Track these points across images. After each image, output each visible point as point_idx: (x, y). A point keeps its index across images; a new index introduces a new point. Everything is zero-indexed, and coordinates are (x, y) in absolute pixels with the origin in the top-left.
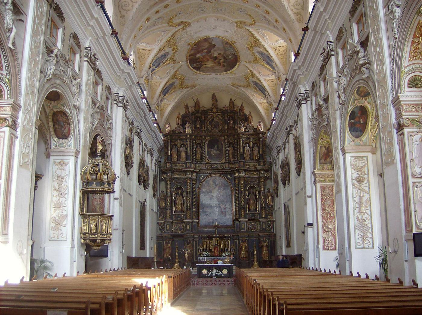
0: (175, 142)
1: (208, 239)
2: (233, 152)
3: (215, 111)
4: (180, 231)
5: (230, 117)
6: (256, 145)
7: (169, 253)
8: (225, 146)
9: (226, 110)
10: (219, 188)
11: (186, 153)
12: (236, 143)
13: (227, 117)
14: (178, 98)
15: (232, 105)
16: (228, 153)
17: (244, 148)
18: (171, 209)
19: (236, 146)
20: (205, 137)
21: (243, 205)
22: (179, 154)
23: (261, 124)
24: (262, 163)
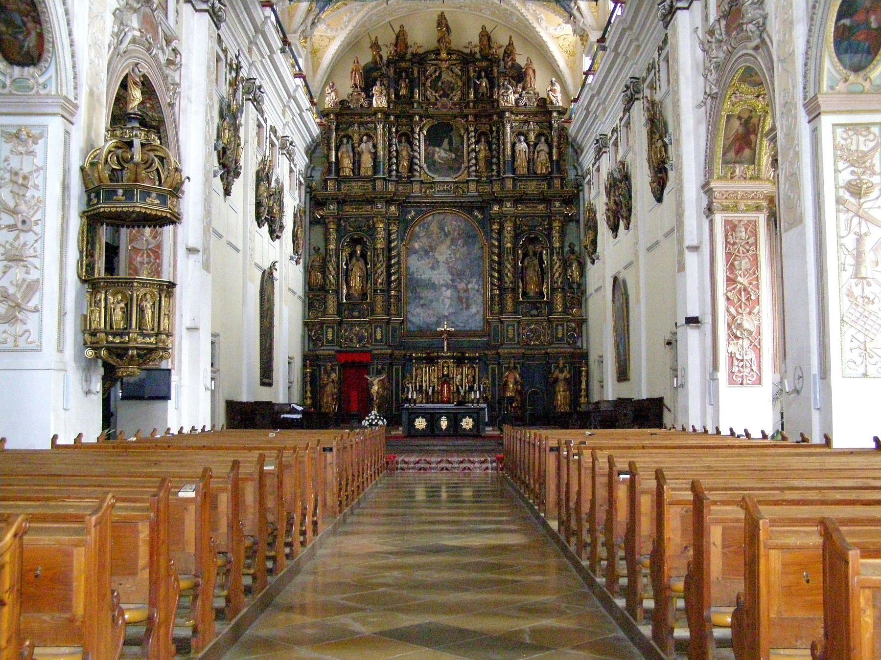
0: (347, 129)
1: (427, 363)
2: (489, 155)
3: (444, 55)
4: (360, 341)
6: (543, 139)
7: (333, 395)
8: (469, 139)
9: (472, 54)
10: (453, 241)
11: (375, 156)
12: (494, 134)
13: (475, 71)
14: (354, 22)
15: (485, 42)
16: (476, 158)
17: (513, 145)
18: (337, 292)
19: (495, 141)
20: (421, 117)
21: (512, 283)
22: (357, 159)
23: (557, 87)
24: (557, 182)
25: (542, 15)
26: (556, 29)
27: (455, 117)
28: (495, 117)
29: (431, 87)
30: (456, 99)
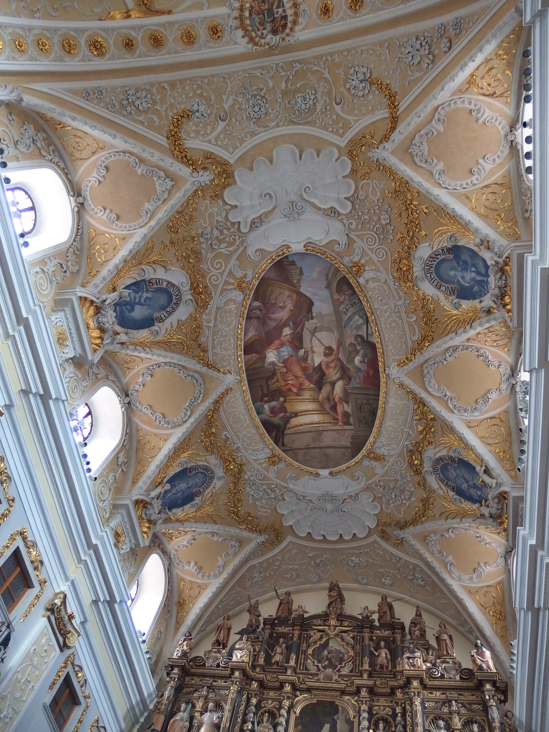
3: (333, 622)
5: (380, 641)
12: (399, 718)
13: (371, 639)
14: (229, 569)
15: (386, 608)
23: (488, 654)
25: (450, 558)
26: (471, 579)
27: (343, 692)
28: (399, 694)
29: (313, 655)
30: (345, 671)
